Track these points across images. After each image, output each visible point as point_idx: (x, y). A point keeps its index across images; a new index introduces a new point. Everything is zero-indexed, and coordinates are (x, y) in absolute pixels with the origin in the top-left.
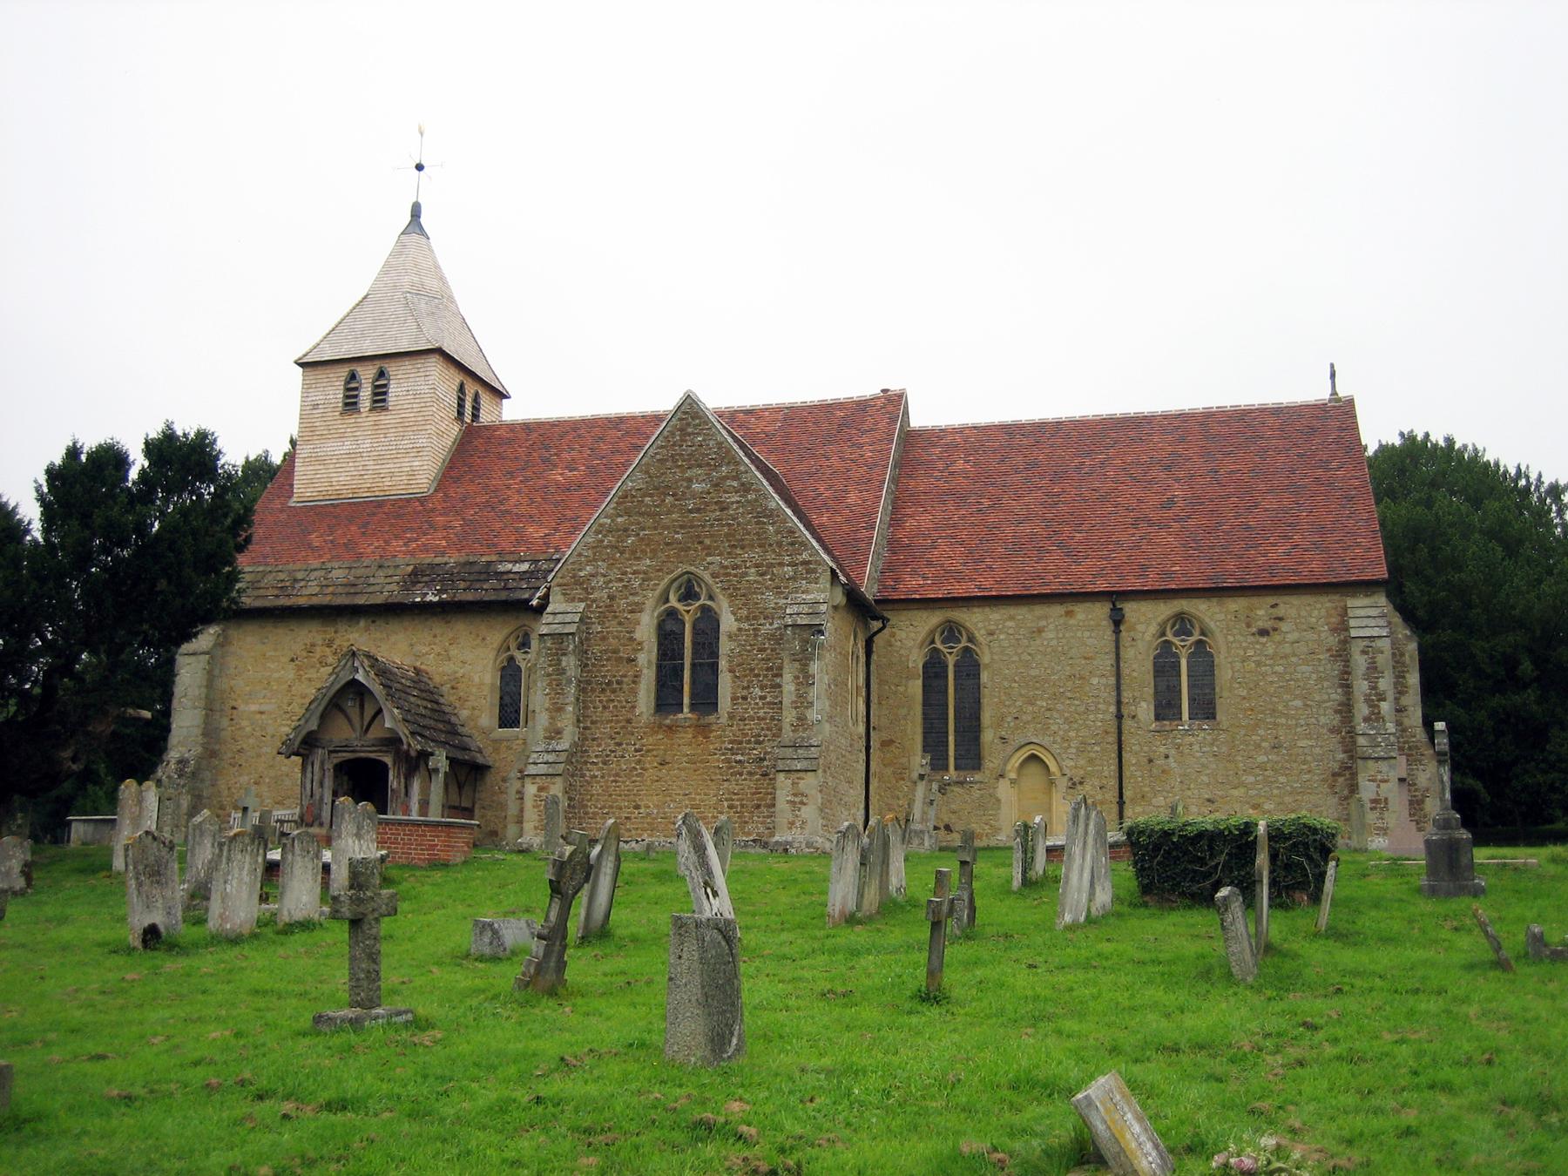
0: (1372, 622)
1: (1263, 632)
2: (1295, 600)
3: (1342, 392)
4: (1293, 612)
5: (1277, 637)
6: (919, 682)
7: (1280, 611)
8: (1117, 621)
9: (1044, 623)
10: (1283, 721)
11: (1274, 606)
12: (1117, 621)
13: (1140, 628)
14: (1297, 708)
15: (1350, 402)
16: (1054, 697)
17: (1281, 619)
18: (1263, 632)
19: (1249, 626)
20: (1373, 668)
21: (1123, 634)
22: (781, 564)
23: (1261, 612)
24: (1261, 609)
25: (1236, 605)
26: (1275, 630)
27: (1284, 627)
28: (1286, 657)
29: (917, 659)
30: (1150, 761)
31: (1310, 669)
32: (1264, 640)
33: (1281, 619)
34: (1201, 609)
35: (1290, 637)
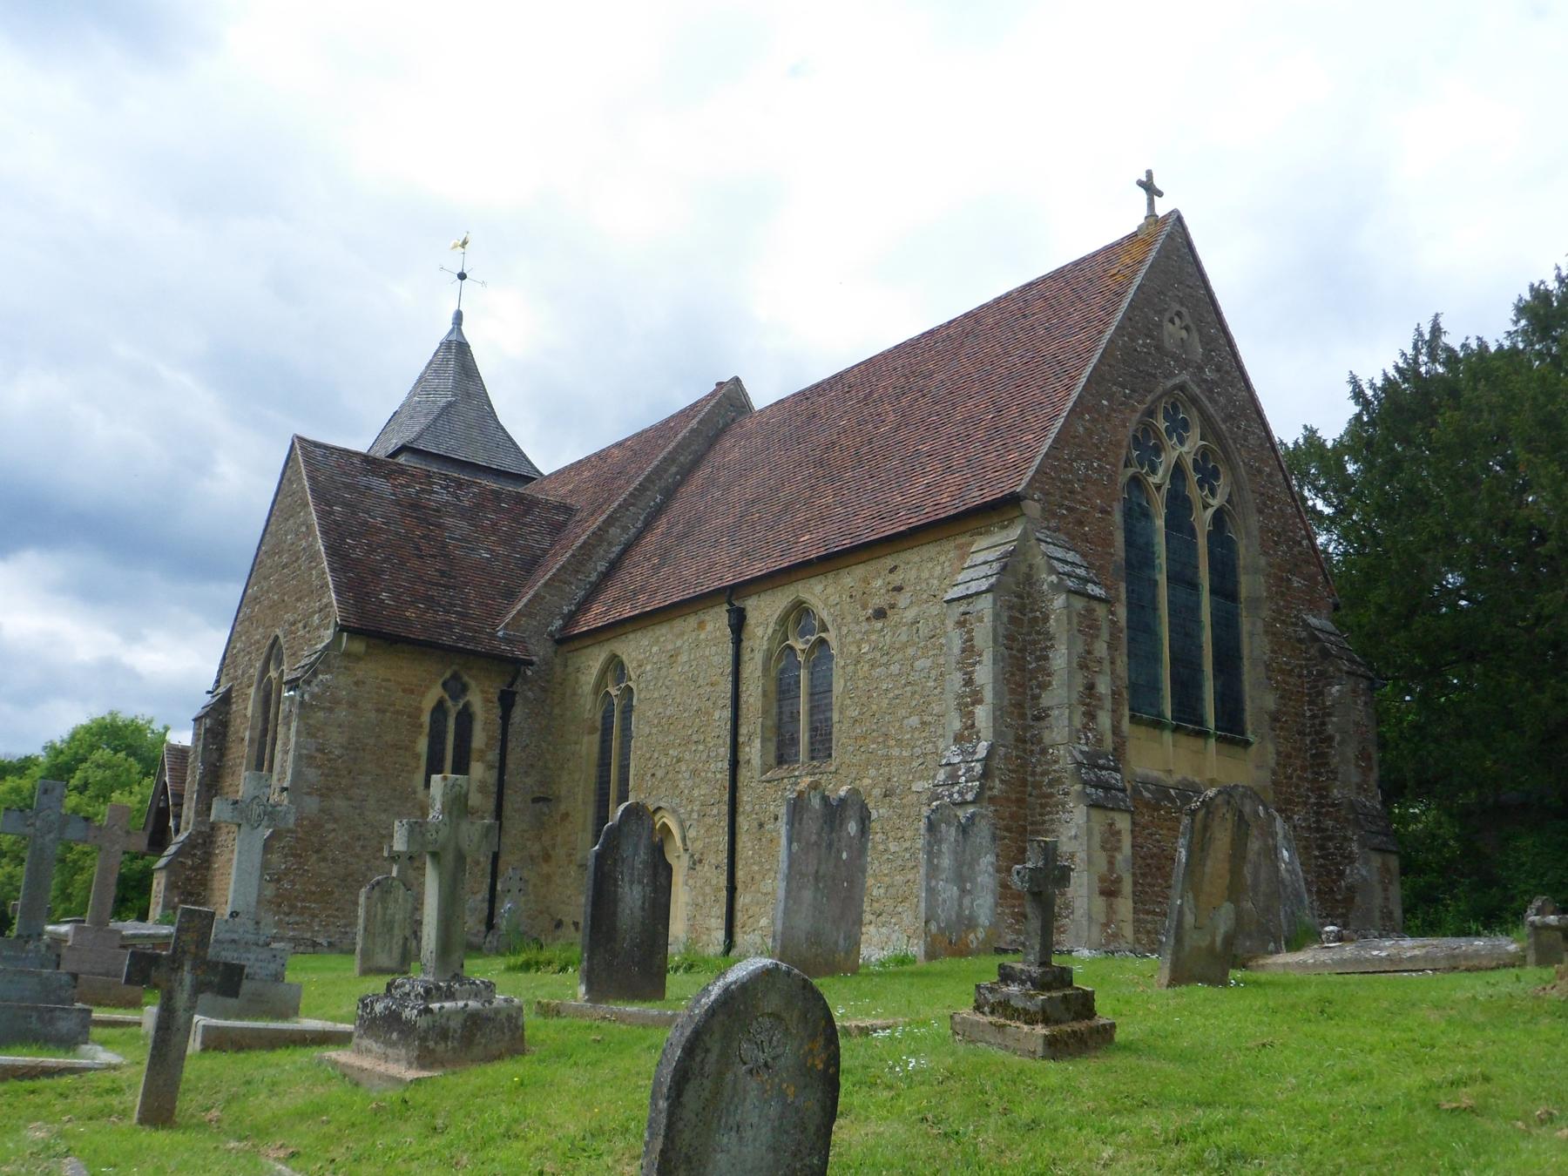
0: (985, 570)
1: (880, 614)
2: (913, 556)
3: (1162, 208)
4: (913, 574)
5: (893, 618)
6: (597, 737)
7: (897, 579)
8: (738, 622)
9: (679, 643)
10: (895, 752)
11: (891, 571)
12: (738, 622)
13: (759, 631)
14: (914, 729)
15: (1177, 219)
16: (687, 741)
17: (899, 589)
18: (880, 614)
19: (864, 607)
20: (969, 649)
21: (744, 644)
22: (314, 613)
23: (879, 582)
24: (872, 579)
25: (851, 578)
26: (892, 606)
27: (903, 600)
28: (905, 646)
29: (587, 705)
30: (761, 825)
31: (928, 663)
32: (879, 625)
33: (899, 589)
34: (819, 594)
35: (910, 614)
